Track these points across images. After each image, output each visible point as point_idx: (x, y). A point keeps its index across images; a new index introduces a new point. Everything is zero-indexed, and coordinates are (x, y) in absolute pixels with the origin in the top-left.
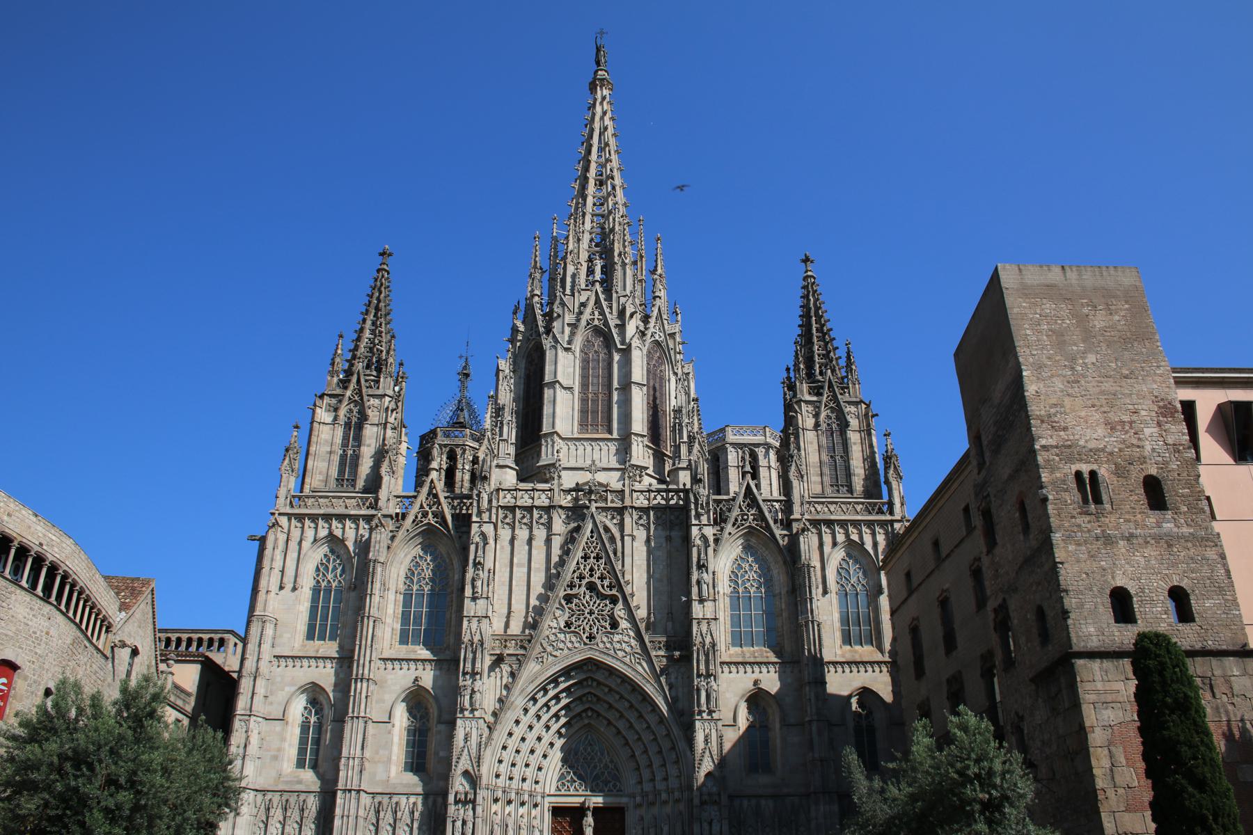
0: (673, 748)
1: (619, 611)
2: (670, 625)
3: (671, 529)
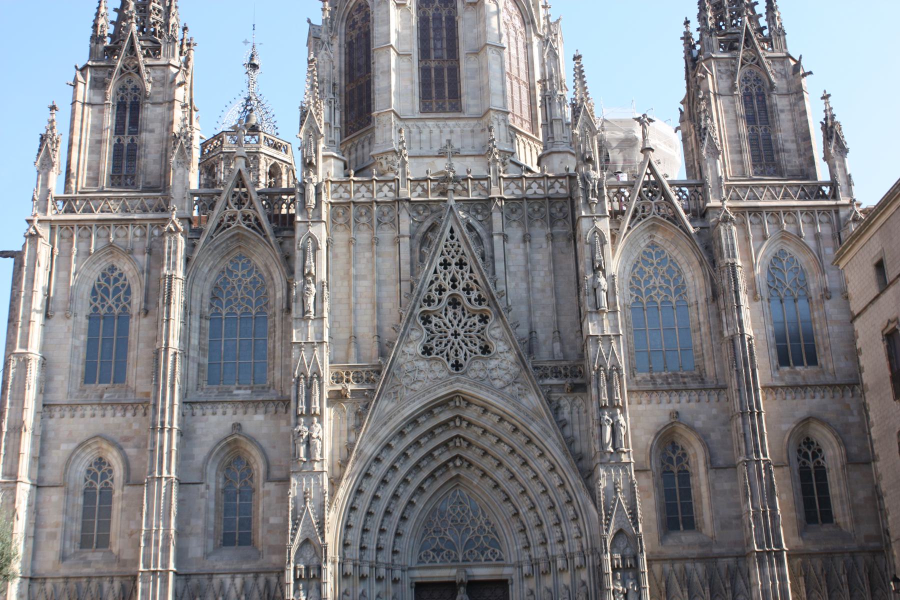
0: (570, 502)
1: (494, 331)
2: (557, 346)
3: (552, 224)
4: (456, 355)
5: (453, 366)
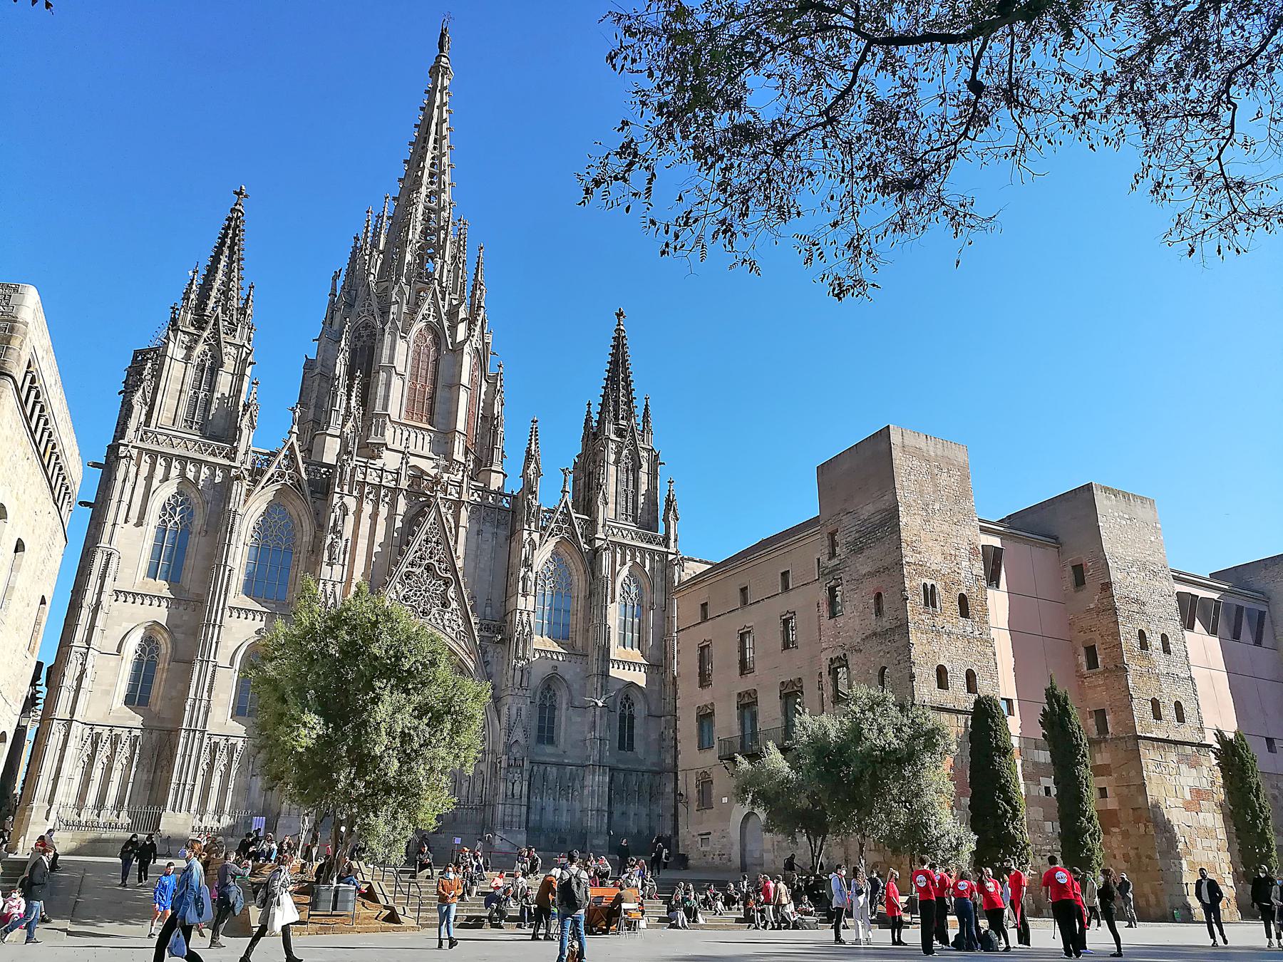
1: (451, 593)
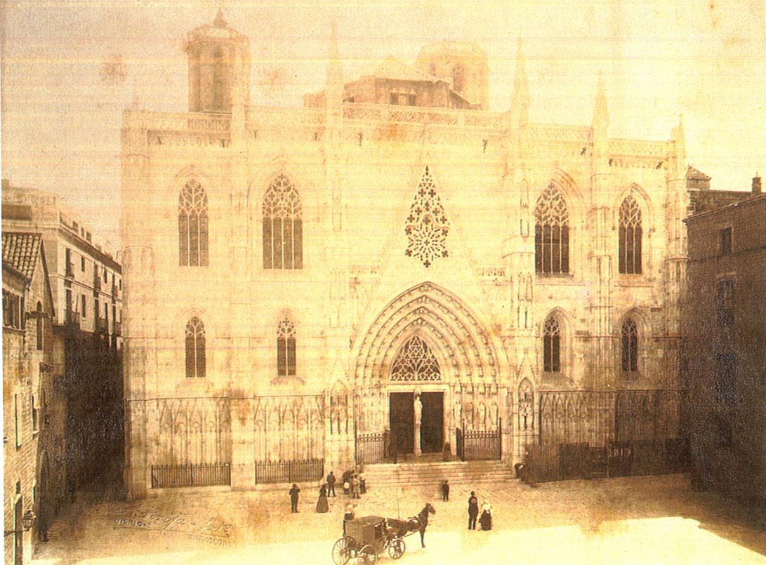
4: (427, 257)
5: (424, 264)
